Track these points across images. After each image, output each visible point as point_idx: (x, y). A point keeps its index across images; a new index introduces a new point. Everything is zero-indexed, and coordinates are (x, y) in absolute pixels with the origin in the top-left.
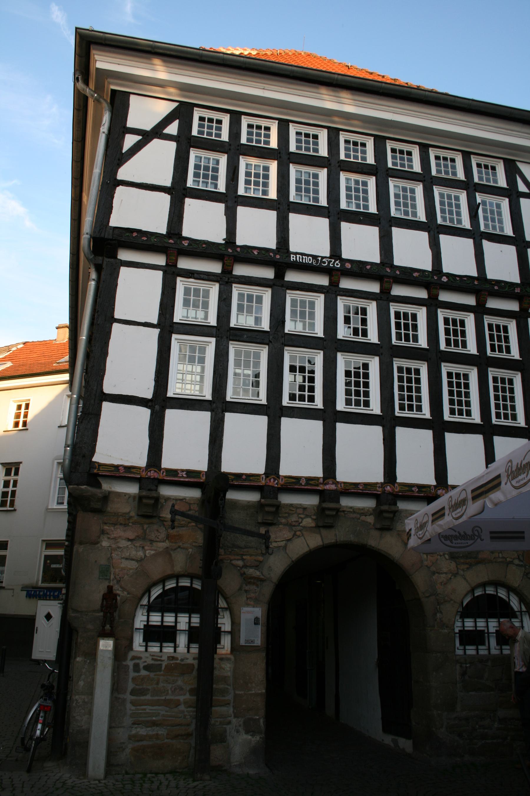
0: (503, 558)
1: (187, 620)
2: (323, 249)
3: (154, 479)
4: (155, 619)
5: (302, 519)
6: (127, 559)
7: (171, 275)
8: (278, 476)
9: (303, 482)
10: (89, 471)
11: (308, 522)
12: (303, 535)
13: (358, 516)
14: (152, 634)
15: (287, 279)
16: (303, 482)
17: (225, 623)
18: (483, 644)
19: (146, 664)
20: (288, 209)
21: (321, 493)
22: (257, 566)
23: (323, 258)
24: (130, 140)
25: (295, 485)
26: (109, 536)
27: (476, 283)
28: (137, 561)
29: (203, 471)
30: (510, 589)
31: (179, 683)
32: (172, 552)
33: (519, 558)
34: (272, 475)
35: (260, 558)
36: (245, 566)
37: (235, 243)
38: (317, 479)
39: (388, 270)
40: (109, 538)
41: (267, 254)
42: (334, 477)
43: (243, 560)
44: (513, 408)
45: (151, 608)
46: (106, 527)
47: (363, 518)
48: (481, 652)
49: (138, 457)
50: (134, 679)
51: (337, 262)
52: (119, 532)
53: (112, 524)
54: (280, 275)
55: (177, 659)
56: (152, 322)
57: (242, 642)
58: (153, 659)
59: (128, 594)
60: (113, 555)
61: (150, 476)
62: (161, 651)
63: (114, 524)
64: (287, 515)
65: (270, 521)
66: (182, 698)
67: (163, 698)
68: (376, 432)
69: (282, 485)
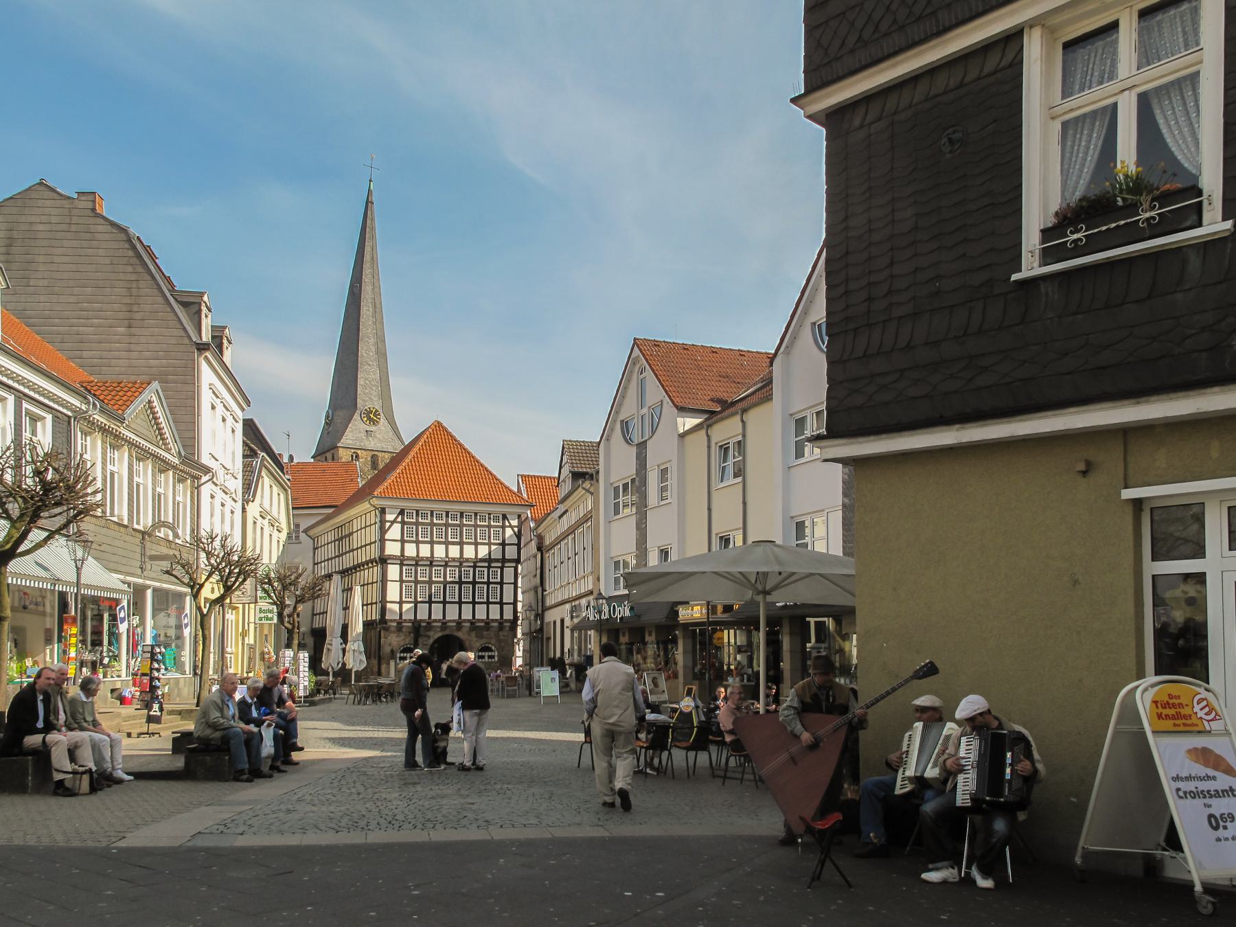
7: (402, 565)
24: (388, 524)
25: (435, 621)
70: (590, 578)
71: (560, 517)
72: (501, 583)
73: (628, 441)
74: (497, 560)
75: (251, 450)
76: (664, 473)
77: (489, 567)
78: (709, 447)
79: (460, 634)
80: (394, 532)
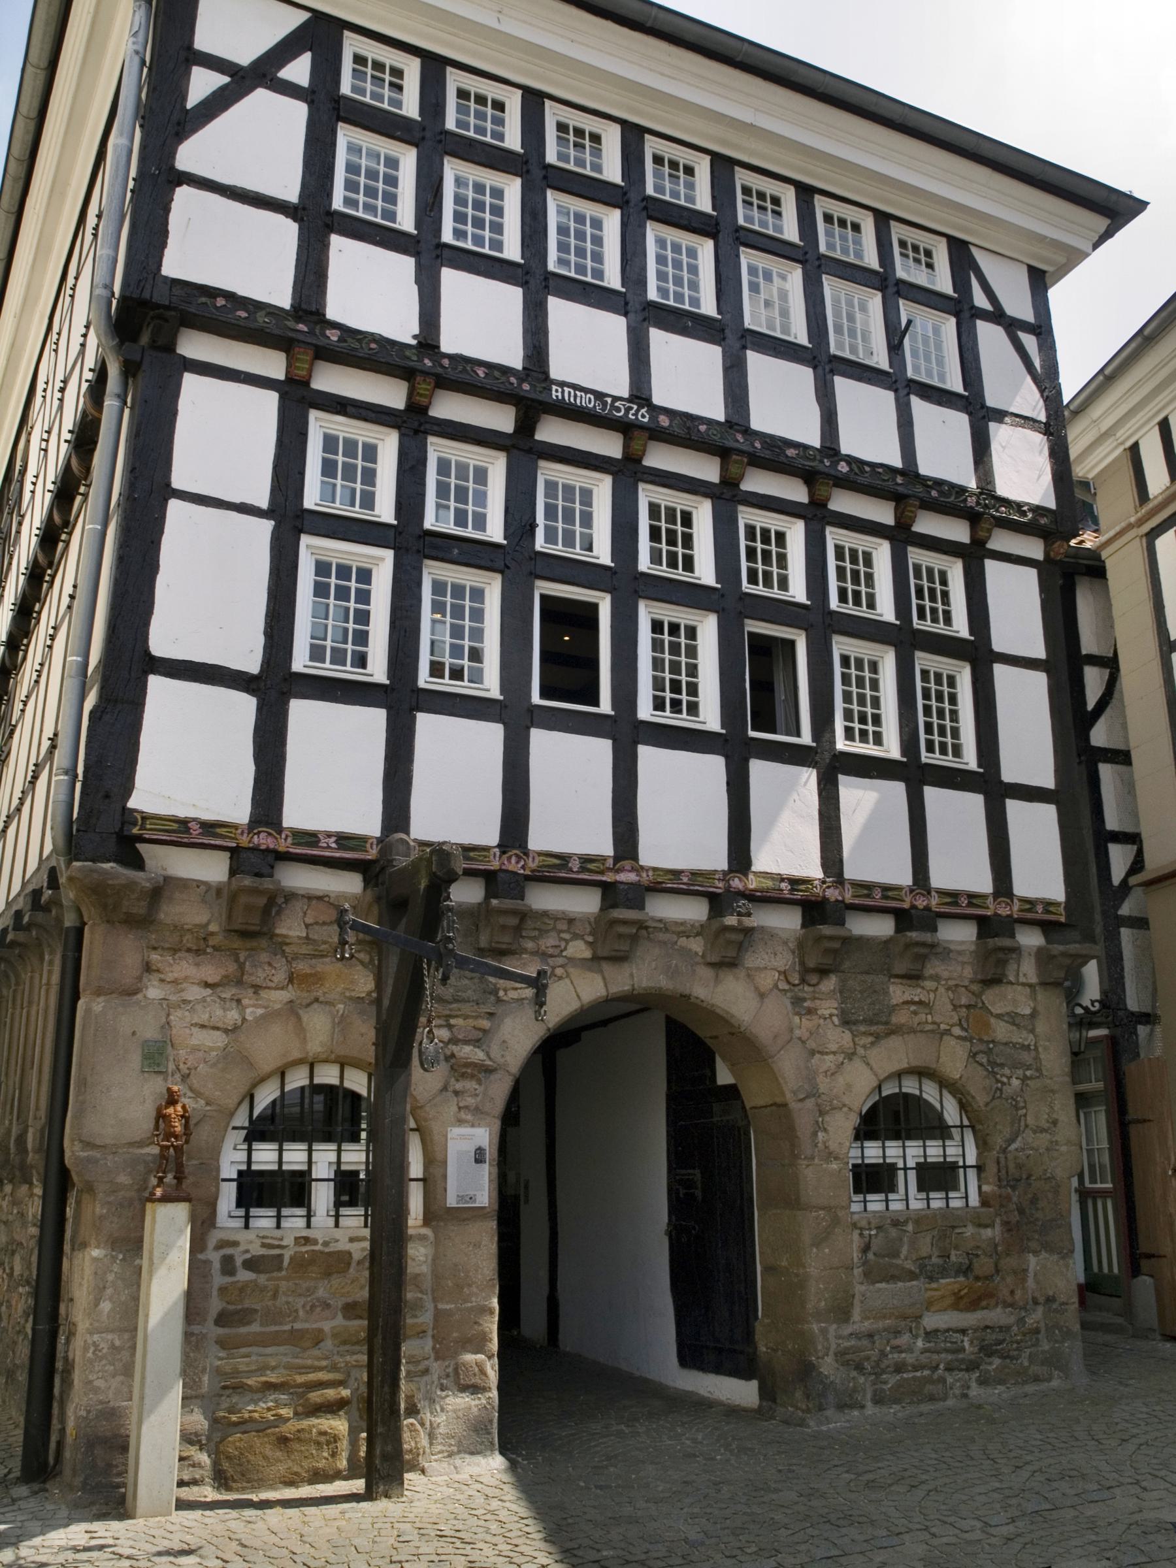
0: (934, 1023)
1: (333, 1157)
2: (616, 381)
3: (268, 851)
4: (265, 1156)
5: (567, 942)
6: (203, 1026)
7: (297, 400)
8: (526, 853)
9: (575, 865)
10: (122, 829)
11: (579, 949)
12: (568, 976)
13: (675, 938)
14: (258, 1190)
15: (538, 437)
16: (575, 865)
18: (956, 1188)
19: (248, 1256)
20: (546, 287)
21: (608, 889)
22: (478, 1040)
23: (616, 399)
26: (162, 976)
27: (899, 480)
28: (226, 1031)
29: (372, 837)
30: (944, 1084)
31: (321, 1293)
32: (301, 1012)
33: (960, 1025)
34: (514, 848)
35: (485, 1024)
36: (454, 1041)
37: (438, 347)
38: (602, 859)
39: (740, 437)
40: (162, 981)
41: (503, 379)
42: (635, 857)
43: (450, 1027)
44: (956, 733)
45: (257, 1132)
46: (155, 957)
47: (683, 941)
48: (893, 1206)
50: (223, 1290)
51: (643, 411)
52: (184, 967)
53: (169, 949)
54: (526, 426)
55: (315, 1242)
56: (257, 504)
57: (452, 1201)
58: (264, 1245)
59: (207, 1104)
60: (172, 1017)
61: (259, 845)
62: (278, 1226)
63: (174, 951)
64: (537, 933)
65: (504, 946)
66: (327, 1326)
67: (287, 1327)
68: (714, 767)
69: (533, 871)
80: (260, 141)
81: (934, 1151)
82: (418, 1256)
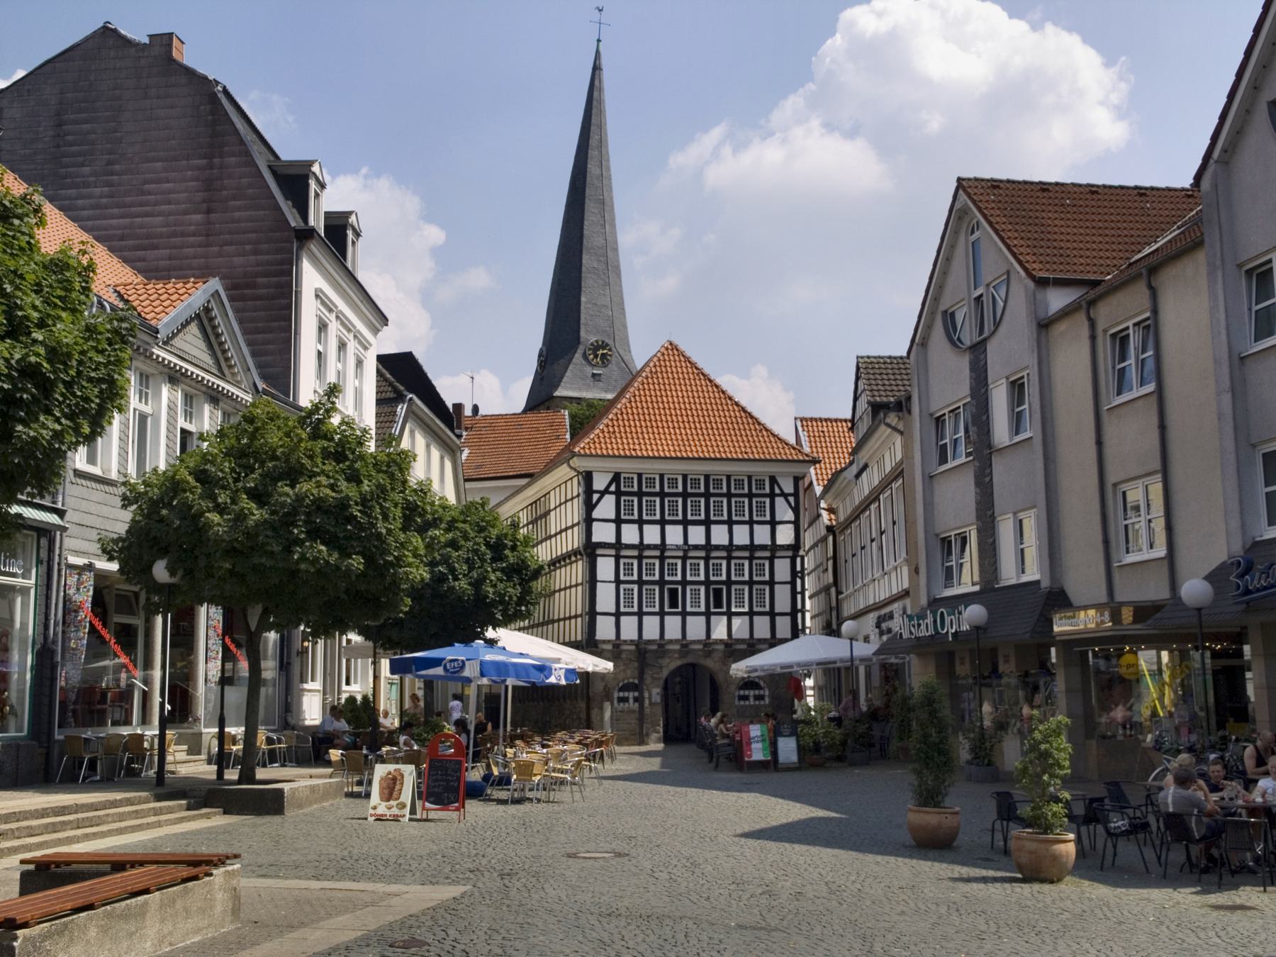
2: (680, 541)
4: (621, 694)
7: (618, 558)
14: (621, 700)
17: (646, 695)
24: (596, 497)
25: (671, 642)
49: (612, 636)
54: (662, 552)
70: (905, 570)
71: (858, 475)
72: (772, 583)
73: (954, 342)
74: (763, 547)
75: (395, 390)
76: (1017, 389)
77: (751, 559)
78: (1093, 338)
79: (709, 663)
80: (606, 508)
81: (757, 692)
82: (647, 711)
